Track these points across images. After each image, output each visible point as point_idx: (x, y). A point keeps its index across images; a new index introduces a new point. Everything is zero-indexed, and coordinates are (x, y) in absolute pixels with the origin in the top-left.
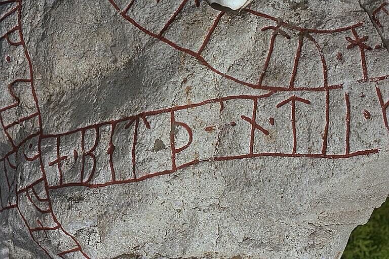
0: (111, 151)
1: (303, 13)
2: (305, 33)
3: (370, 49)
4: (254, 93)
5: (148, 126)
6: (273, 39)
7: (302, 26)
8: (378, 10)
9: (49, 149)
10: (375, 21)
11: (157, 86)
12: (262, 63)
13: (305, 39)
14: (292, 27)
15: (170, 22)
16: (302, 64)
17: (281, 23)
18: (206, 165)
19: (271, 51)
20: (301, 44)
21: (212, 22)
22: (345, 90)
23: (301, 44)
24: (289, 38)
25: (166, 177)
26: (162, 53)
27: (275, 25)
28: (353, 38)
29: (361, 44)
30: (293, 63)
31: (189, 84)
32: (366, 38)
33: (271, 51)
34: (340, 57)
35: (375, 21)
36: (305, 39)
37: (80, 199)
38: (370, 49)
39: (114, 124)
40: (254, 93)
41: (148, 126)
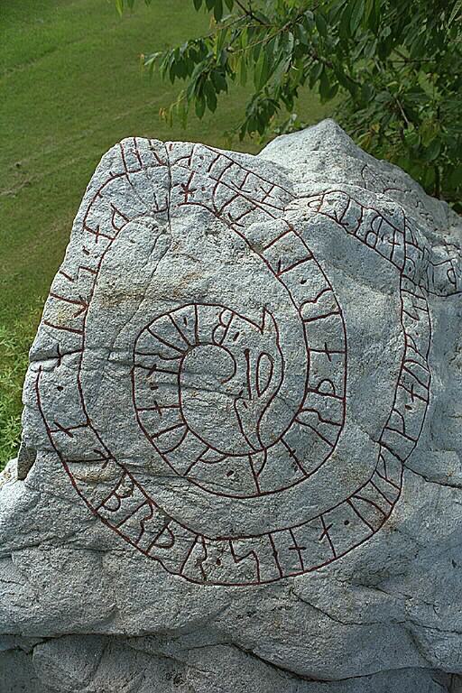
0: (360, 221)
1: (211, 227)
2: (218, 214)
3: (183, 185)
4: (263, 205)
5: (335, 213)
6: (239, 218)
7: (217, 219)
8: (161, 211)
9: (399, 254)
10: (167, 203)
11: (322, 228)
12: (251, 214)
13: (219, 209)
14: (223, 221)
15: (303, 261)
16: (228, 198)
17: (230, 226)
18: (303, 194)
19: (242, 215)
20: (223, 207)
21: (275, 244)
22: (208, 174)
23: (223, 207)
24: (229, 214)
25: (329, 190)
26: (314, 245)
27: (234, 225)
28: (189, 195)
29: (186, 190)
30: (233, 202)
31: (303, 217)
32: (181, 193)
33: (242, 215)
34: (203, 189)
35: (167, 203)
36: (219, 209)
37: (386, 211)
38: (183, 185)
39: (355, 235)
40: (263, 205)
41: (335, 213)
